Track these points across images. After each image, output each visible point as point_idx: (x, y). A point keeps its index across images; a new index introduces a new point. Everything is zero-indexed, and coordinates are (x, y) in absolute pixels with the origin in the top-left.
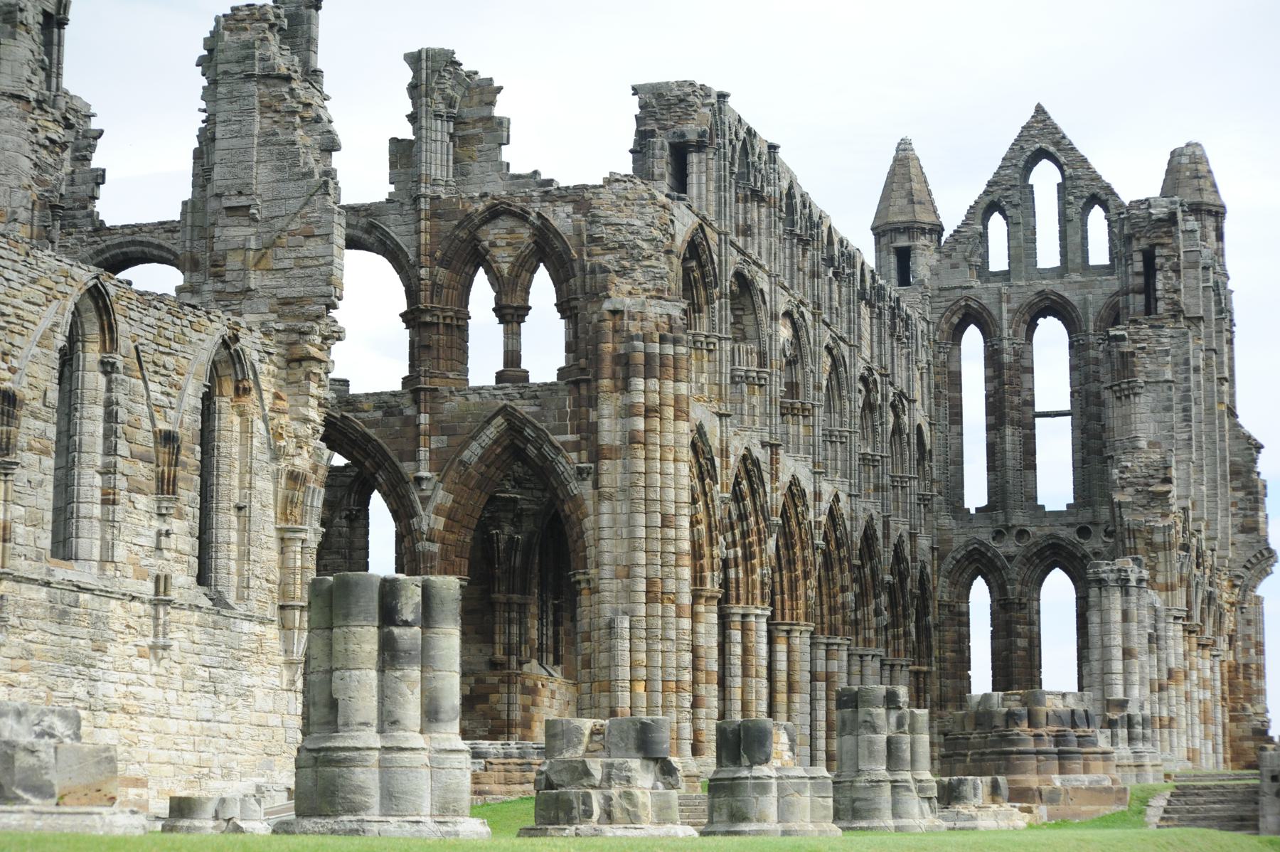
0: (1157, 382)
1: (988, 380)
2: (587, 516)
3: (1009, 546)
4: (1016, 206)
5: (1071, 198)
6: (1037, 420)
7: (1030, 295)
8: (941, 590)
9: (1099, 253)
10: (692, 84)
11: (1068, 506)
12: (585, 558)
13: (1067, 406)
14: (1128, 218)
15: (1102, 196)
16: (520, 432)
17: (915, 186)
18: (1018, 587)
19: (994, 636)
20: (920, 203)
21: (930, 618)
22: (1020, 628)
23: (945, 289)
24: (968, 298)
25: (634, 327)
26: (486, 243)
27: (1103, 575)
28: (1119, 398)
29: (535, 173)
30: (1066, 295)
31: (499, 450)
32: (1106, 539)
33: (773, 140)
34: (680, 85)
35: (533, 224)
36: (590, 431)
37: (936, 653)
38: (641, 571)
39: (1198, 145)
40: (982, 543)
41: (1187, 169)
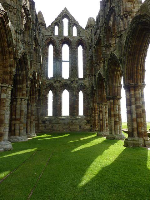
1: (54, 54)
3: (57, 84)
8: (43, 92)
13: (68, 60)
15: (76, 24)
19: (53, 102)
21: (41, 97)
23: (47, 36)
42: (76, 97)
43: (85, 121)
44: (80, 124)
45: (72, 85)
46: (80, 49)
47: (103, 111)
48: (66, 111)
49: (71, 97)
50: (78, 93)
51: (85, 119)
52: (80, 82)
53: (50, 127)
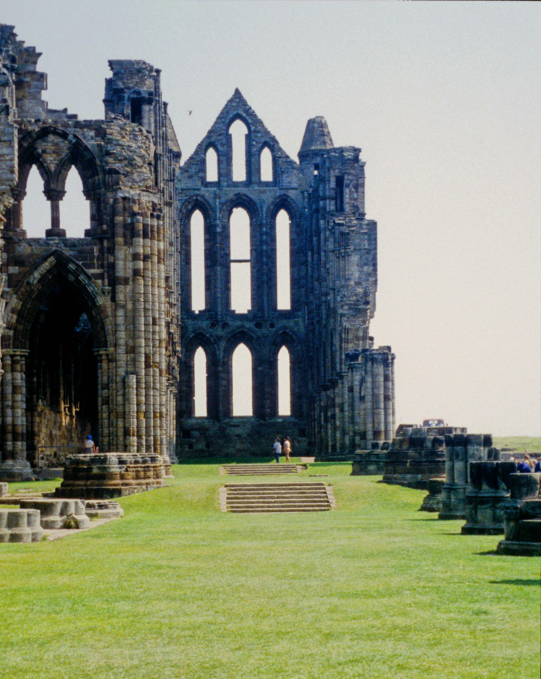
0: (360, 250)
2: (107, 317)
5: (254, 143)
7: (231, 196)
9: (267, 173)
10: (144, 63)
11: (249, 311)
12: (106, 342)
13: (248, 257)
14: (329, 158)
15: (271, 143)
16: (65, 266)
19: (208, 379)
24: (197, 195)
25: (136, 208)
26: (40, 151)
27: (376, 356)
28: (338, 258)
29: (65, 110)
30: (251, 196)
31: (50, 277)
33: (167, 101)
34: (138, 62)
35: (70, 142)
36: (112, 267)
38: (143, 350)
39: (322, 117)
41: (315, 130)
45: (263, 330)
46: (283, 220)
48: (242, 404)
50: (276, 353)
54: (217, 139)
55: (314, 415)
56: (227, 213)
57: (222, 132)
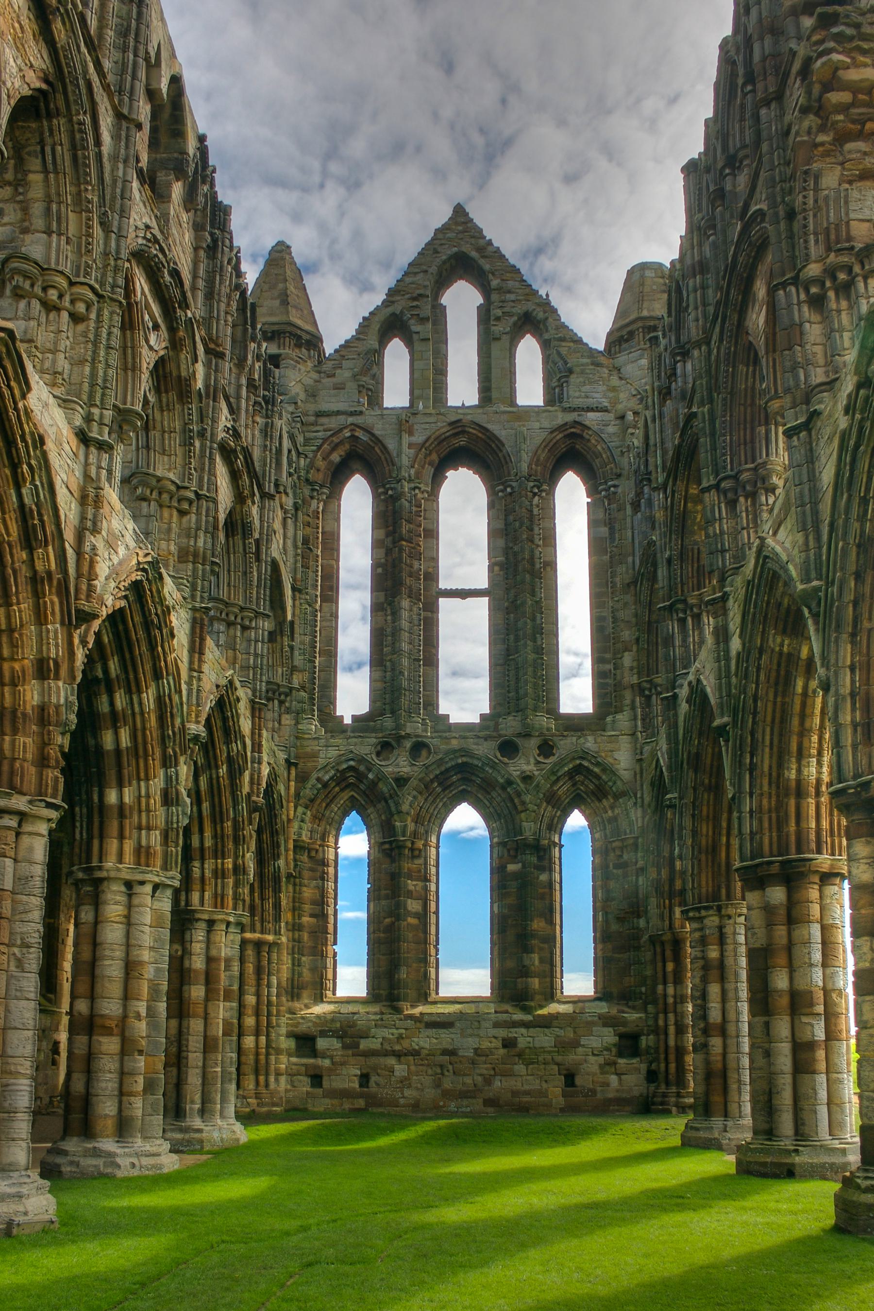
3: (400, 764)
4: (423, 320)
6: (442, 601)
7: (441, 427)
9: (530, 389)
17: (291, 288)
18: (411, 826)
20: (295, 307)
21: (281, 862)
22: (411, 884)
32: (541, 759)
37: (287, 916)
40: (361, 760)
42: (540, 858)
43: (608, 1037)
44: (571, 1058)
47: (729, 961)
49: (500, 857)
50: (556, 825)
51: (607, 1021)
52: (566, 745)
53: (348, 1078)
54: (410, 315)
55: (665, 996)
56: (429, 471)
57: (421, 291)
